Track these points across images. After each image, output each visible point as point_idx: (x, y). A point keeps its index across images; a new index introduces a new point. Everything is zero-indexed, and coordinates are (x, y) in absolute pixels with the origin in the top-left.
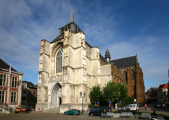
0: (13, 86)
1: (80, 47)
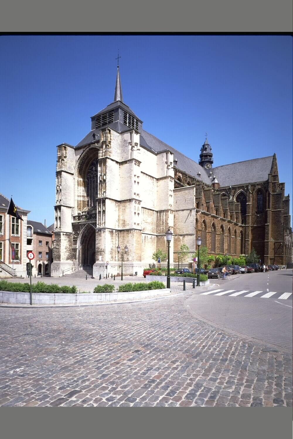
0: (13, 233)
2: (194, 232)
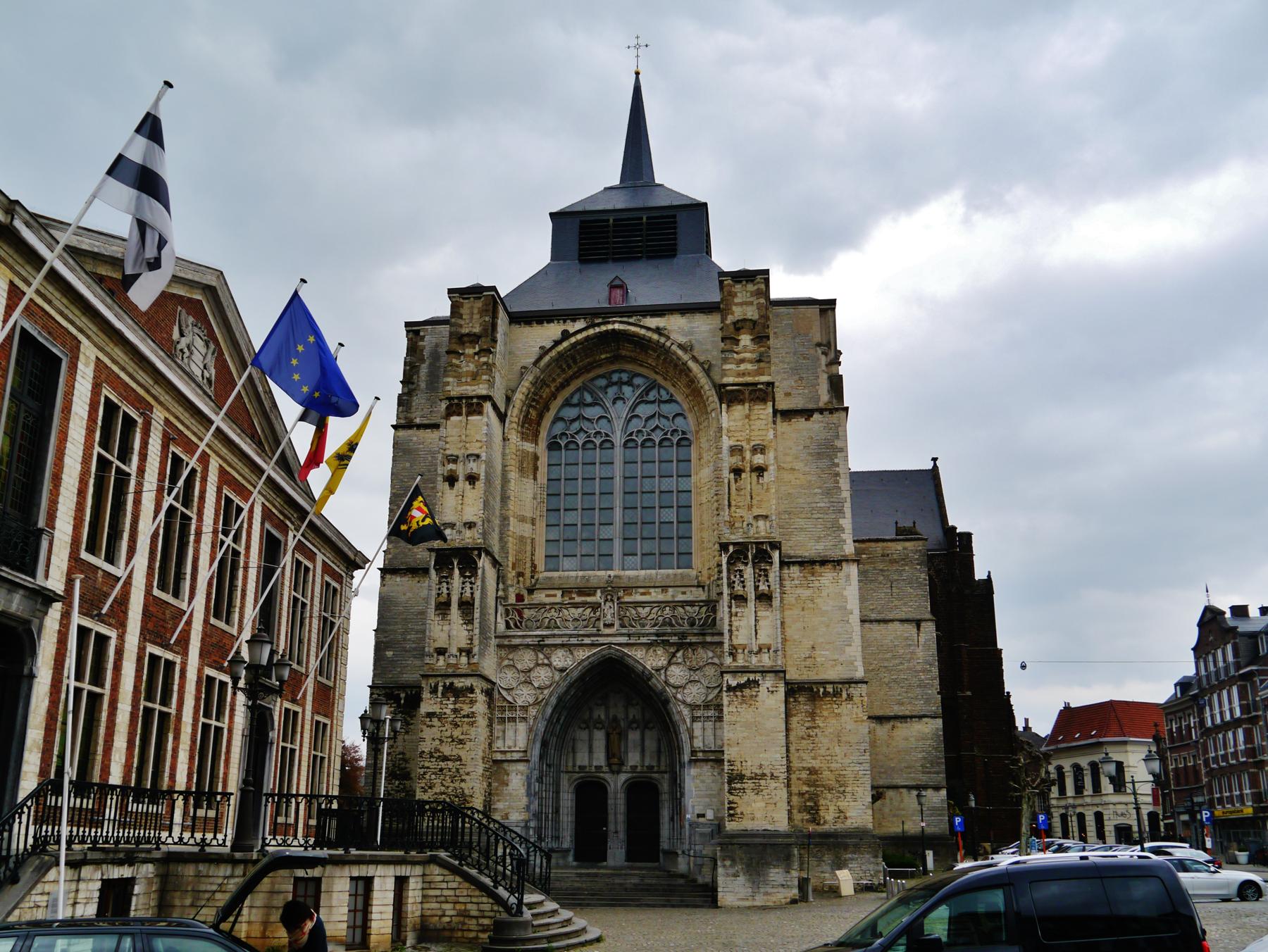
2: (935, 706)
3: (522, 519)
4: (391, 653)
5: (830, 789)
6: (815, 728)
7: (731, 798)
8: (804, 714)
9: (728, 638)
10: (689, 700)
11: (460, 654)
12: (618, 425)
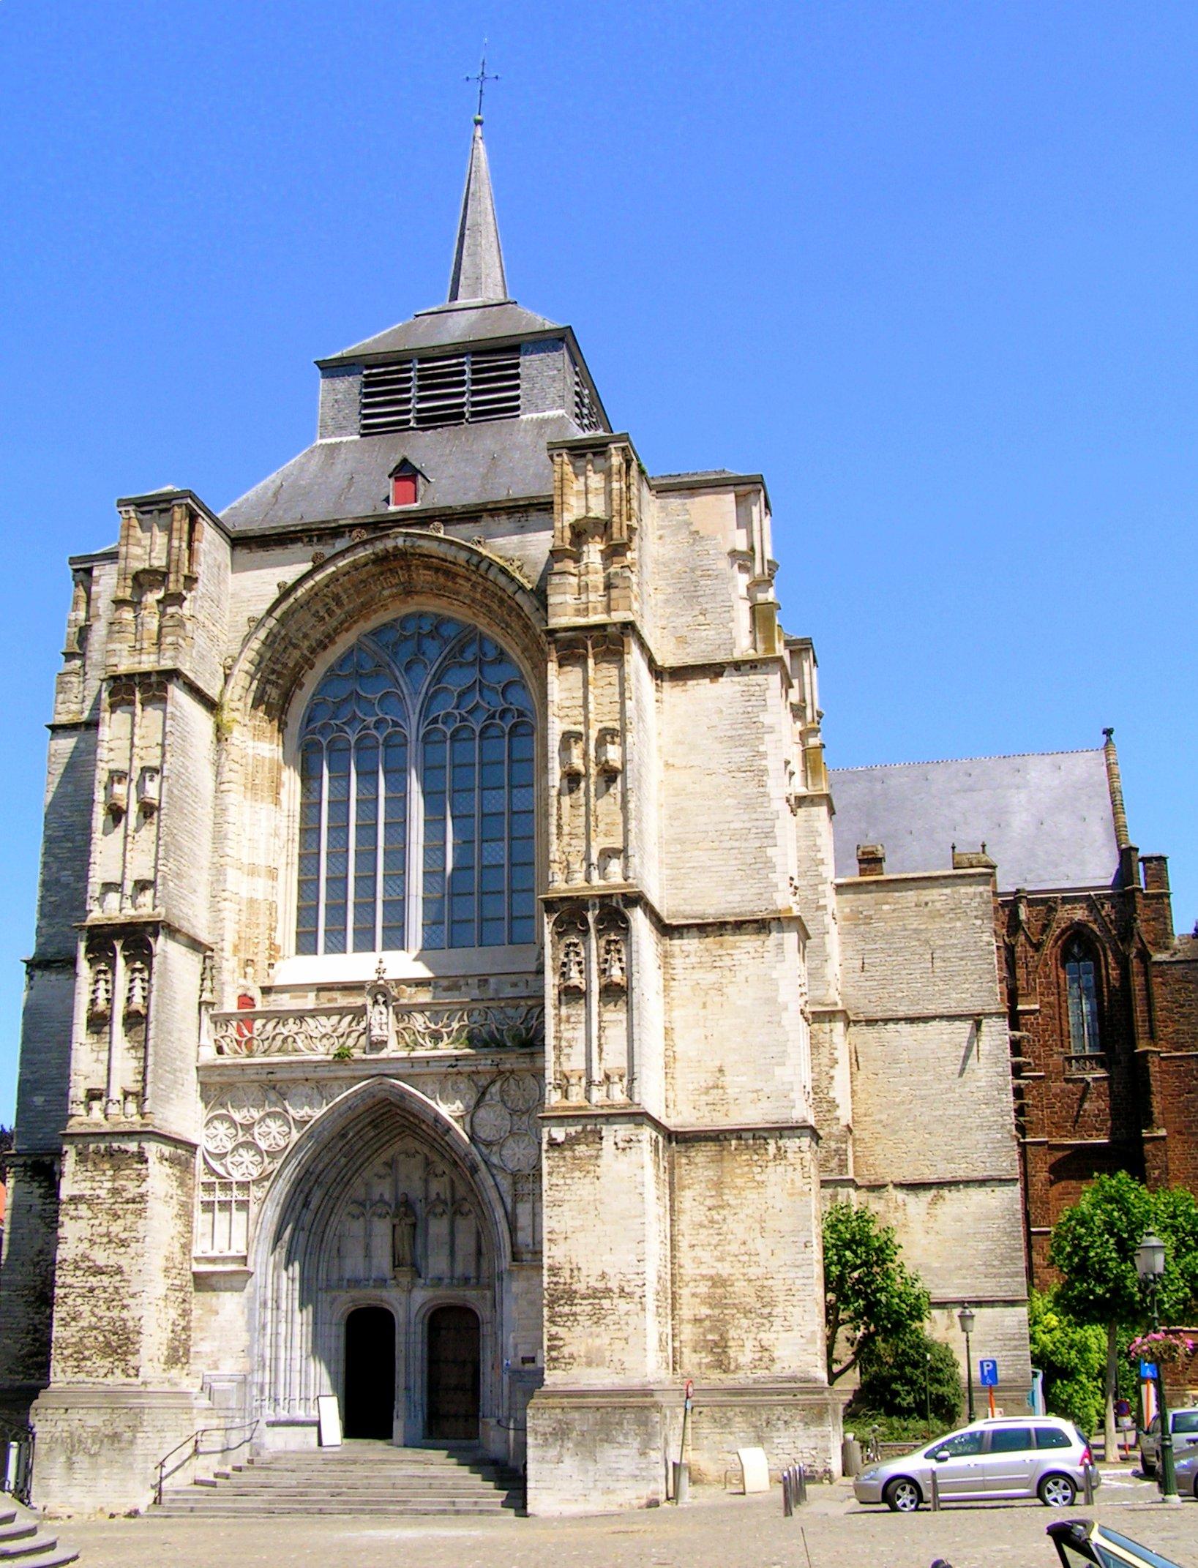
1: (738, 666)
2: (1009, 1164)
3: (253, 871)
4: (42, 1099)
5: (747, 1312)
6: (722, 1207)
7: (554, 1330)
8: (703, 1185)
9: (553, 1059)
10: (511, 1166)
11: (125, 1099)
12: (414, 706)
